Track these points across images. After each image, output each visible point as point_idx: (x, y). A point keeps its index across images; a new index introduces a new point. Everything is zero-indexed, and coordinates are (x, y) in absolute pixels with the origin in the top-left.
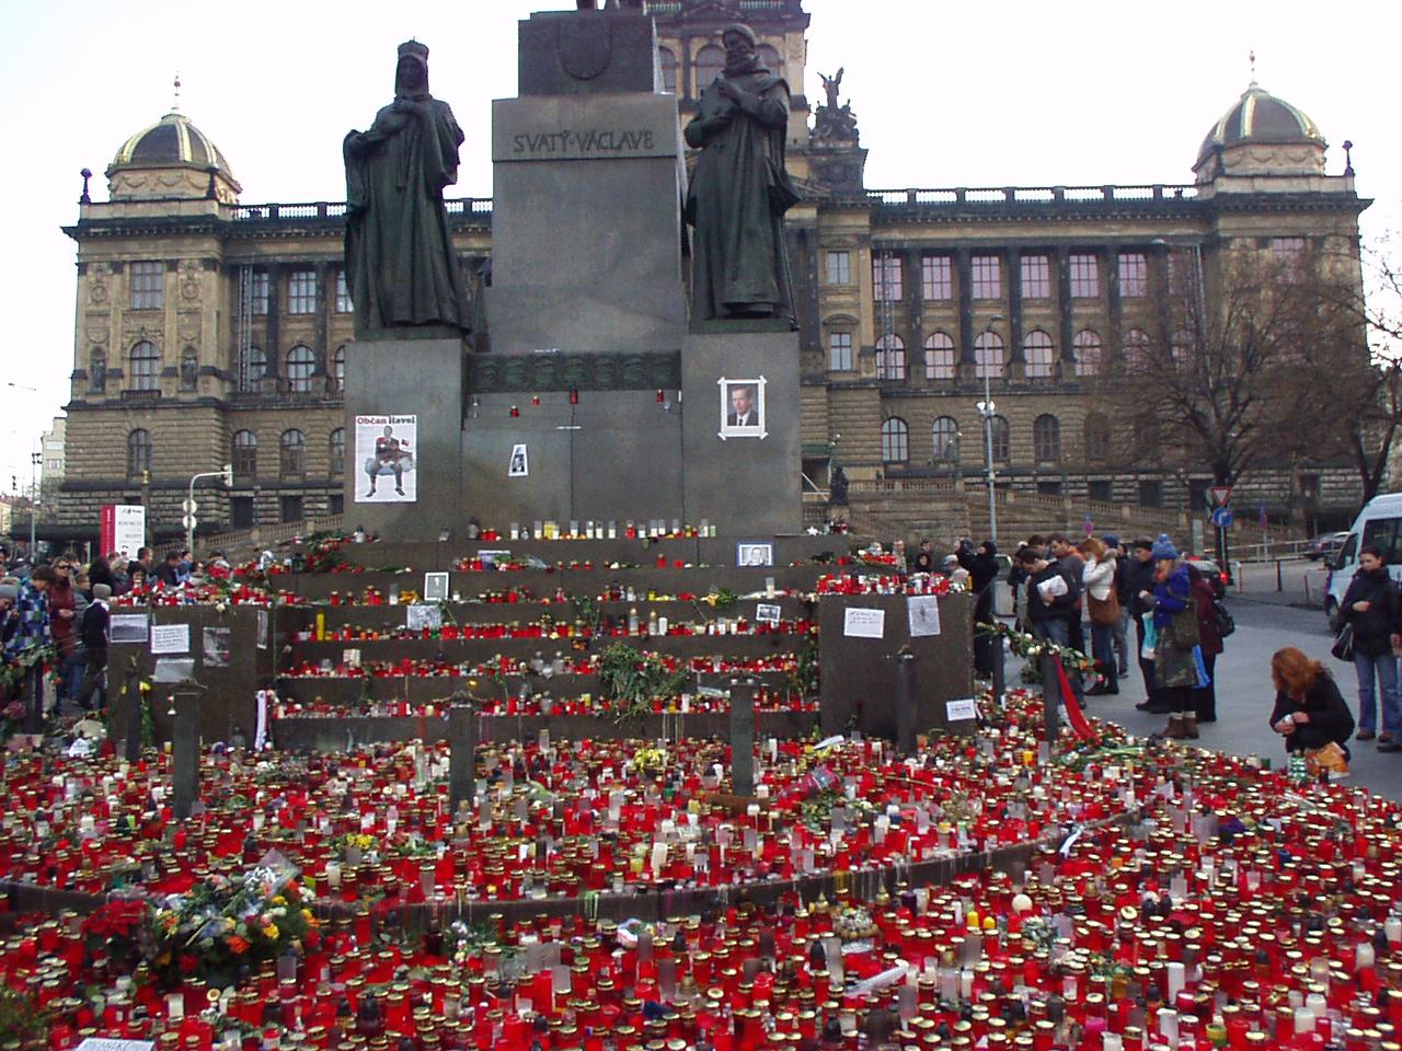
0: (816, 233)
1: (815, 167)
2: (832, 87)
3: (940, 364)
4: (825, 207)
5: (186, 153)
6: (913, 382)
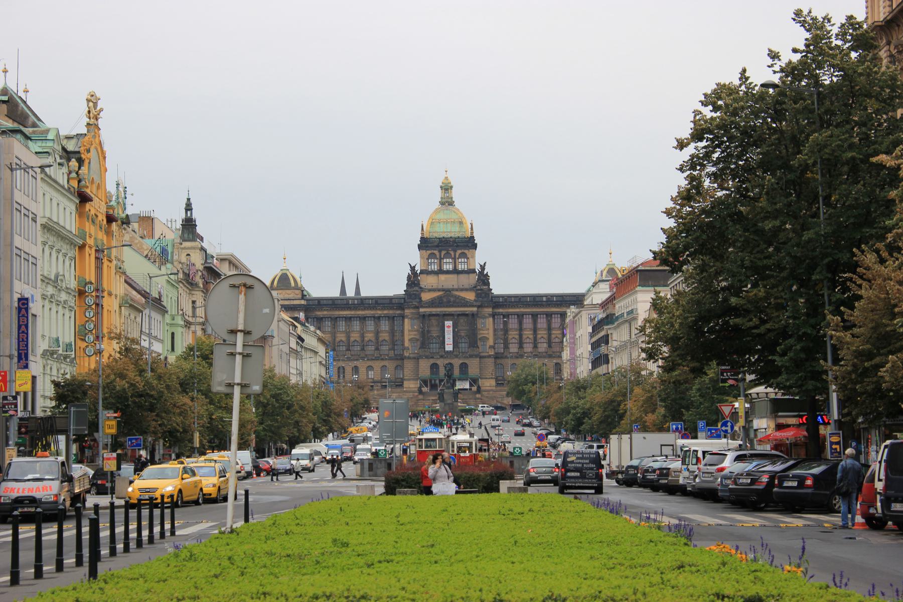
0: (477, 314)
1: (477, 296)
2: (483, 267)
3: (514, 348)
4: (479, 307)
5: (293, 284)
6: (505, 354)
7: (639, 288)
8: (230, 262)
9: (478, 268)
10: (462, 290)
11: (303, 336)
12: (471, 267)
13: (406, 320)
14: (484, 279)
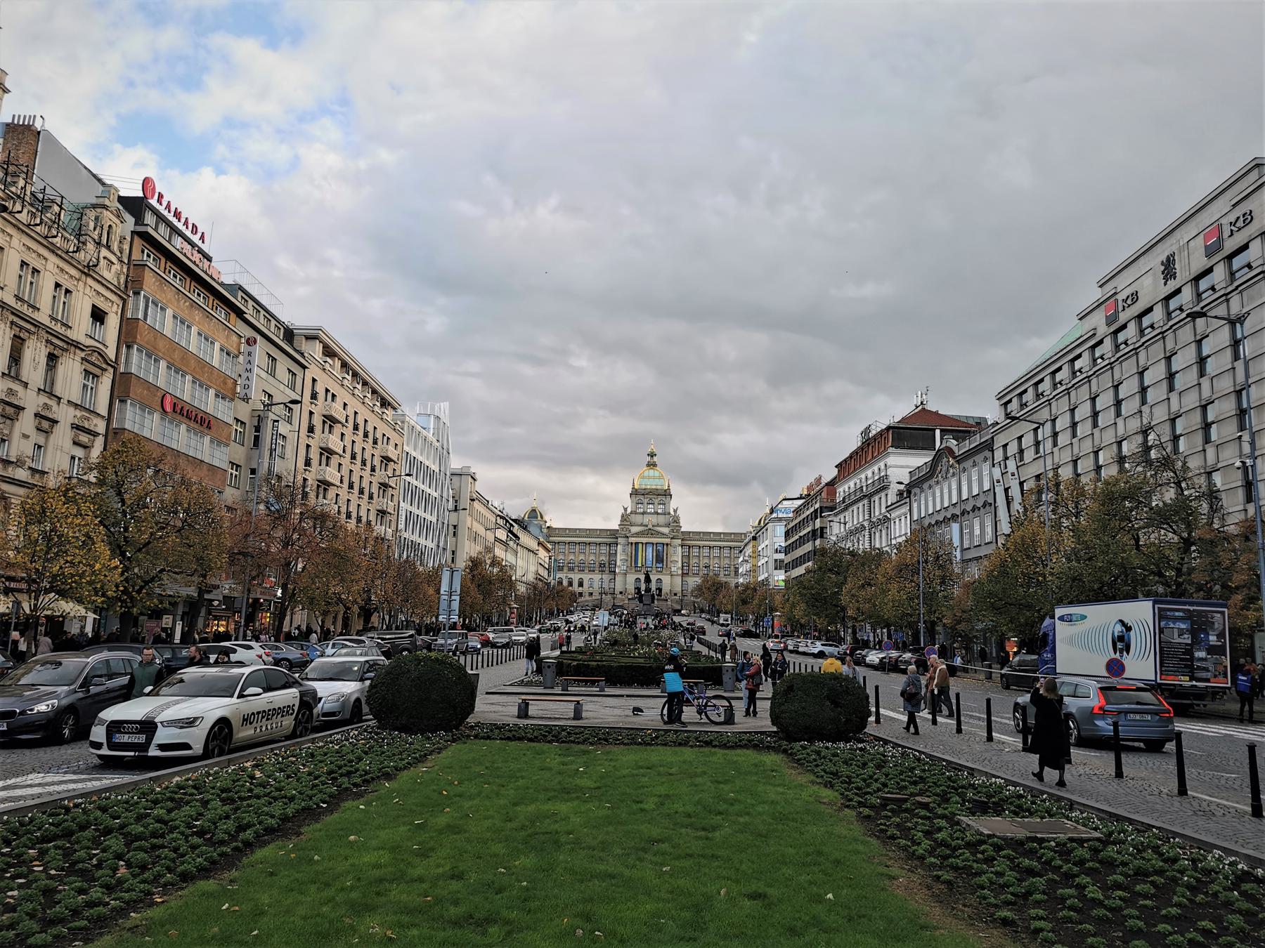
2: (675, 511)
7: (891, 450)
8: (329, 352)
9: (672, 513)
10: (661, 526)
11: (520, 534)
12: (667, 511)
13: (619, 546)
14: (676, 520)
